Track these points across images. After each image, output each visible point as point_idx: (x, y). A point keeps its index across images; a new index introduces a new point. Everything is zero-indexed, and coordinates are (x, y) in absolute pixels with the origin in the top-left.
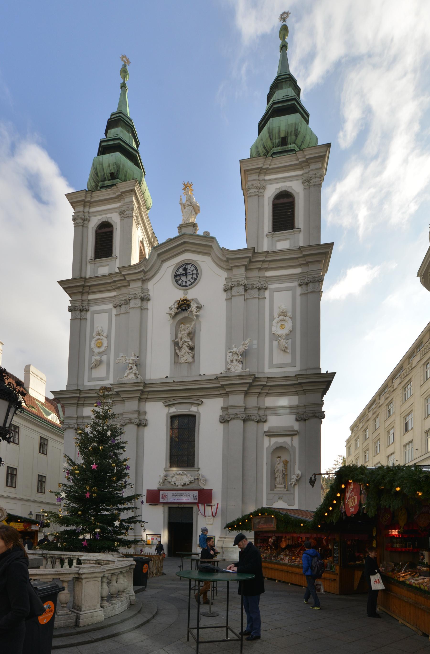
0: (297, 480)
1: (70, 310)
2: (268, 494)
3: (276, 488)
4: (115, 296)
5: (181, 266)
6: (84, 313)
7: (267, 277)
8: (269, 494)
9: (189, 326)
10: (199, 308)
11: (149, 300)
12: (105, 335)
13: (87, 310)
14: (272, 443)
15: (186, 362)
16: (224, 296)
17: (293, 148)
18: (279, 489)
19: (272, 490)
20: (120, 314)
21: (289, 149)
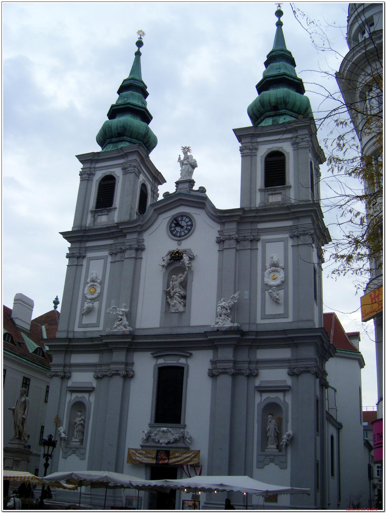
1: (68, 256)
2: (258, 455)
6: (80, 259)
7: (258, 229)
8: (259, 455)
9: (181, 275)
10: (191, 259)
11: (143, 249)
12: (99, 281)
13: (84, 257)
14: (263, 399)
15: (177, 311)
16: (216, 247)
17: (284, 113)
18: (270, 450)
19: (263, 450)
21: (281, 113)
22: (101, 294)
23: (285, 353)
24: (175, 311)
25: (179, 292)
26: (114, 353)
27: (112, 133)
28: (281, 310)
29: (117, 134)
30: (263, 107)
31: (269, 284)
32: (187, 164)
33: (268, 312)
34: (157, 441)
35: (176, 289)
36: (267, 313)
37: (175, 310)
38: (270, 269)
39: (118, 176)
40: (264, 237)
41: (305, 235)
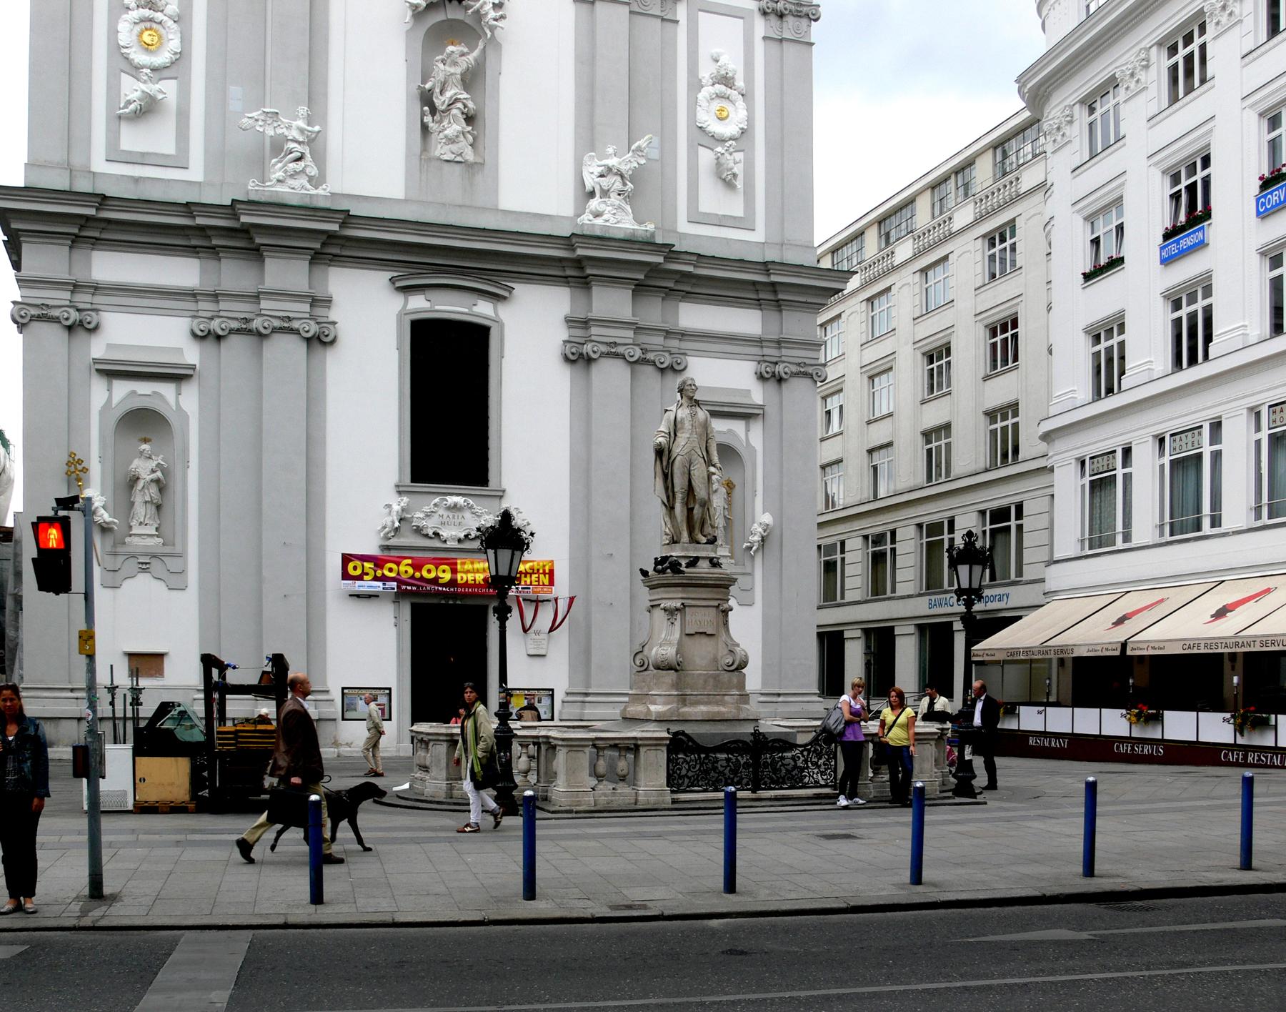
0: (763, 539)
9: (466, 50)
15: (459, 159)
22: (180, 60)
23: (746, 321)
24: (454, 156)
25: (464, 101)
26: (267, 261)
28: (734, 206)
31: (710, 129)
35: (453, 92)
37: (454, 153)
38: (711, 87)
41: (800, 16)
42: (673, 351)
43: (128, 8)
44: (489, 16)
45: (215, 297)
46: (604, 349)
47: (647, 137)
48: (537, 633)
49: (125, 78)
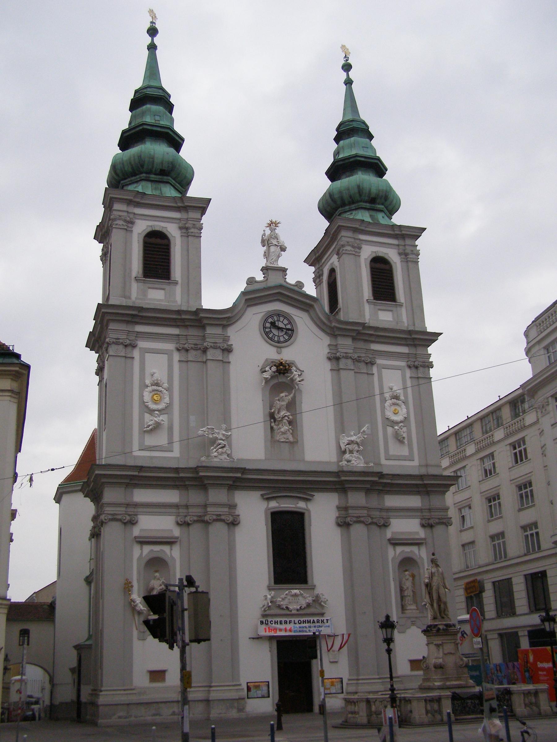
3: (407, 610)
4: (178, 335)
5: (271, 315)
6: (129, 349)
9: (287, 394)
13: (134, 346)
16: (328, 365)
18: (410, 611)
20: (187, 361)
27: (153, 167)
28: (405, 451)
29: (159, 170)
30: (360, 195)
32: (277, 245)
33: (392, 452)
34: (284, 607)
36: (392, 452)
39: (174, 236)
40: (379, 361)
41: (425, 367)
42: (385, 517)
43: (148, 386)
44: (297, 380)
45: (187, 507)
46: (355, 519)
47: (366, 426)
48: (334, 651)
49: (147, 416)
